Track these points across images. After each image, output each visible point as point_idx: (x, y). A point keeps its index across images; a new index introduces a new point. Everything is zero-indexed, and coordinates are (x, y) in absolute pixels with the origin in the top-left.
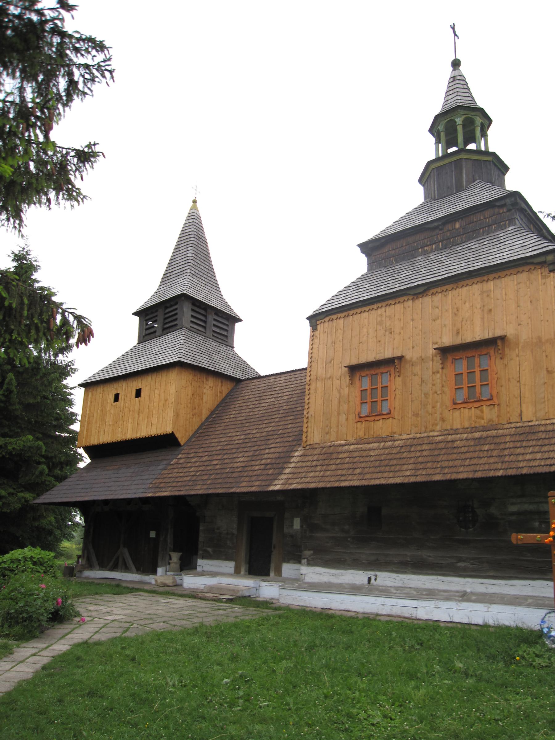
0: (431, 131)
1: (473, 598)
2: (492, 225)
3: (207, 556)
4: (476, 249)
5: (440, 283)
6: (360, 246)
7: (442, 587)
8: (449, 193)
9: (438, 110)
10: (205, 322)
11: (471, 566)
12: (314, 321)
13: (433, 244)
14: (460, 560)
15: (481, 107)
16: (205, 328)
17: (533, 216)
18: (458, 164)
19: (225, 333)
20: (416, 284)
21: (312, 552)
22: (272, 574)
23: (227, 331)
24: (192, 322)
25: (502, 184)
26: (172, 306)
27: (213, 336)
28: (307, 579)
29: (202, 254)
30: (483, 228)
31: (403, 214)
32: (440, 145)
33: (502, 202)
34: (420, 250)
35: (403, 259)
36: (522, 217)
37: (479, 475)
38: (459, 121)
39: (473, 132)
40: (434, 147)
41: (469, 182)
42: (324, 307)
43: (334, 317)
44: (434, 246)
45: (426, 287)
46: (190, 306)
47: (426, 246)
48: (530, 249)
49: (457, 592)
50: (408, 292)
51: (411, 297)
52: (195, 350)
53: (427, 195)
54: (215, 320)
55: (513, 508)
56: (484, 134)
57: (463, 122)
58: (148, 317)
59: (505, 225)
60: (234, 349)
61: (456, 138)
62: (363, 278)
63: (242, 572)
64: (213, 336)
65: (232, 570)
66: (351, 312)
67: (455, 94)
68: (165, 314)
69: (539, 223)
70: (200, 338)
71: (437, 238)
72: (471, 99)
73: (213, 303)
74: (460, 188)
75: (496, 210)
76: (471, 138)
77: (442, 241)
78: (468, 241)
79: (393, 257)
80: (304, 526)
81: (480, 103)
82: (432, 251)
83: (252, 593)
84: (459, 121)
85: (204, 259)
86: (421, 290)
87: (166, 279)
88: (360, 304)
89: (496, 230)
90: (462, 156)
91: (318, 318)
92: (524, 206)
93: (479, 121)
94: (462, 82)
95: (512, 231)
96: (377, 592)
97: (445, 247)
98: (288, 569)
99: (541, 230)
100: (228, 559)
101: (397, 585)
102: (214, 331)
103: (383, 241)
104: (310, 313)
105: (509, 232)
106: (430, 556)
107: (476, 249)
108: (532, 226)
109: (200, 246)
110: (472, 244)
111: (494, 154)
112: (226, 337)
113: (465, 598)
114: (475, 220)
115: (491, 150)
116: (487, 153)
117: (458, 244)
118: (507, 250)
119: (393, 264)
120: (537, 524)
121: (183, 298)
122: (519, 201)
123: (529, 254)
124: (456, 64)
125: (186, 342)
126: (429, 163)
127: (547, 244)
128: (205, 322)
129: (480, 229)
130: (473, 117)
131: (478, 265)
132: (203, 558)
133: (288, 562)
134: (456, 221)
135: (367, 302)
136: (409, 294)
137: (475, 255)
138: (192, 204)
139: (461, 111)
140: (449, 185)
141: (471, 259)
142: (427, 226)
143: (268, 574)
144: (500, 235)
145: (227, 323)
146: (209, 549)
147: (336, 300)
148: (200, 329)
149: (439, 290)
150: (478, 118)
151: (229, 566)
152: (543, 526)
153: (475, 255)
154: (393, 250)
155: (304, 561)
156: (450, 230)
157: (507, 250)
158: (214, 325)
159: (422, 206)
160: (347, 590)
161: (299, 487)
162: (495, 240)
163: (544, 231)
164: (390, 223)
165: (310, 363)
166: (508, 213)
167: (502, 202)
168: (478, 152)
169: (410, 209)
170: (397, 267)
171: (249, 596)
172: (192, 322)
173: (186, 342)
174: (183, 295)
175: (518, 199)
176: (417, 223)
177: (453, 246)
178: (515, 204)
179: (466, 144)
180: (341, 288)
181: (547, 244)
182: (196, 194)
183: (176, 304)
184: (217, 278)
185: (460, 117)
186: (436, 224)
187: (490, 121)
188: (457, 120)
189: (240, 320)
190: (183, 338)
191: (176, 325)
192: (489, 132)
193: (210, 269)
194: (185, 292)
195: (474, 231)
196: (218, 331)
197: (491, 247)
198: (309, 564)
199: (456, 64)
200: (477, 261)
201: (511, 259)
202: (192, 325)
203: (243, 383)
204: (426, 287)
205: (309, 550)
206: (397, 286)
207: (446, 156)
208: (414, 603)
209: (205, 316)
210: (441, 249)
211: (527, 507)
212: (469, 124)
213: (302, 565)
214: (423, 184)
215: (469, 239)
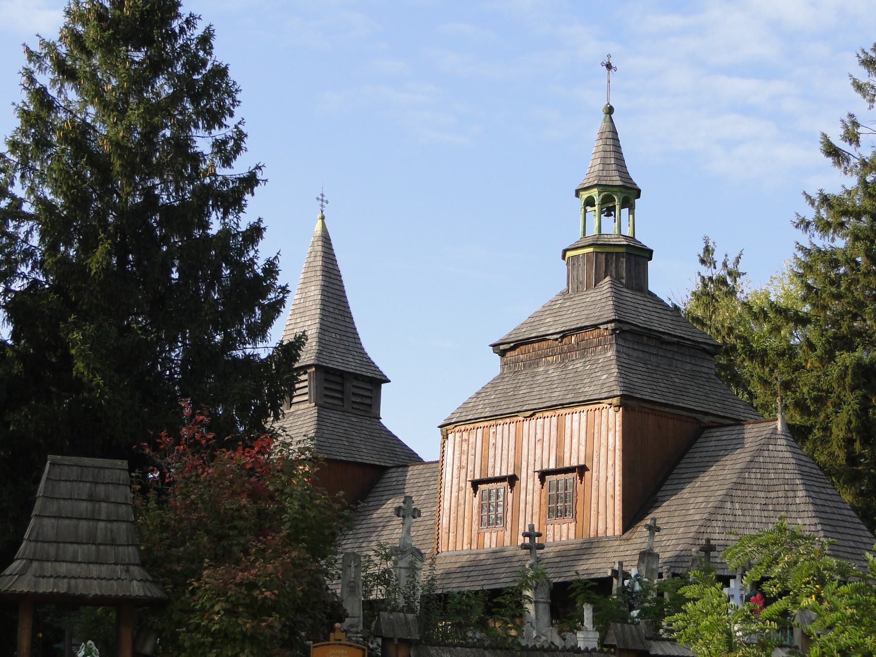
6: (494, 346)
12: (444, 429)
16: (342, 399)
17: (643, 331)
19: (368, 401)
23: (371, 398)
24: (326, 396)
27: (353, 408)
29: (335, 296)
43: (463, 428)
45: (532, 412)
52: (330, 436)
54: (355, 386)
62: (493, 384)
64: (353, 408)
66: (477, 425)
69: (655, 333)
70: (335, 416)
71: (557, 349)
73: (352, 366)
77: (560, 354)
99: (660, 337)
102: (353, 402)
108: (645, 338)
109: (331, 286)
112: (370, 405)
128: (342, 392)
142: (547, 337)
148: (336, 402)
149: (540, 415)
158: (354, 394)
163: (666, 337)
167: (605, 326)
172: (326, 396)
182: (322, 206)
186: (555, 337)
187: (639, 191)
189: (389, 381)
193: (346, 314)
196: (359, 400)
199: (610, 110)
204: (532, 412)
209: (342, 385)
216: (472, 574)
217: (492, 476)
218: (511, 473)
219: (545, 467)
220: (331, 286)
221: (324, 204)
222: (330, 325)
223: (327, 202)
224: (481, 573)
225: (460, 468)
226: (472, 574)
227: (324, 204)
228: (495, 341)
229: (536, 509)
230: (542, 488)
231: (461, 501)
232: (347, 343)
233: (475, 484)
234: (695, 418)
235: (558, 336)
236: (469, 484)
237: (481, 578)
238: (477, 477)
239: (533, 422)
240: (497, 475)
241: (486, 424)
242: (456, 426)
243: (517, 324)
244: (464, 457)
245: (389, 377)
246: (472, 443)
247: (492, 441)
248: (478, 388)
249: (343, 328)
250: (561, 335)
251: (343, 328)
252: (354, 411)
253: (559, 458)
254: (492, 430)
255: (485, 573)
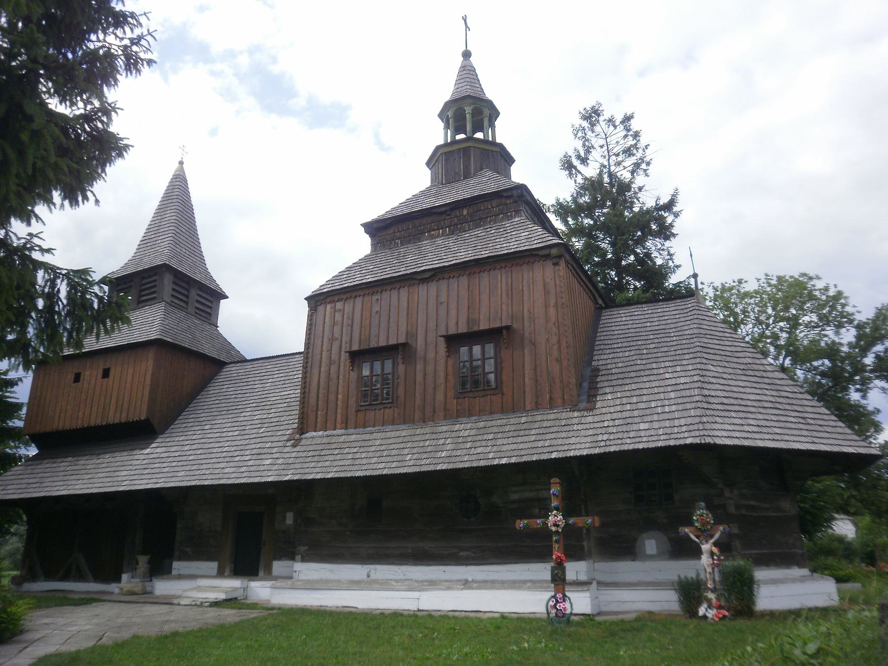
0: (441, 116)
1: (475, 585)
2: (499, 215)
3: (186, 557)
4: (483, 237)
5: (447, 269)
7: (443, 576)
8: (457, 179)
9: (447, 96)
10: (187, 297)
11: (473, 555)
13: (439, 229)
14: (462, 549)
15: (490, 98)
16: (187, 303)
18: (466, 151)
19: (208, 310)
20: (422, 269)
21: (306, 547)
22: (261, 573)
23: (211, 308)
24: (173, 296)
25: (508, 176)
26: (150, 277)
27: (196, 313)
28: (302, 577)
30: (490, 217)
31: (410, 196)
32: (449, 132)
33: (509, 193)
34: (427, 234)
35: (409, 242)
36: (528, 209)
37: (483, 463)
38: (468, 110)
39: (482, 121)
40: (442, 132)
41: (476, 171)
42: (325, 287)
43: (336, 298)
44: (441, 231)
45: (432, 273)
46: (172, 277)
47: (433, 231)
48: (536, 242)
49: (459, 581)
50: (414, 277)
51: (417, 282)
52: (176, 327)
53: (434, 179)
54: (198, 295)
55: (515, 497)
56: (492, 125)
57: (472, 110)
58: (119, 288)
59: (511, 216)
60: (218, 328)
61: (466, 126)
62: (366, 259)
63: (226, 574)
64: (196, 313)
65: (214, 571)
67: (466, 83)
68: (142, 285)
70: (181, 314)
71: (444, 223)
72: (480, 90)
74: (467, 176)
75: (503, 200)
76: (478, 127)
78: (476, 228)
79: (398, 239)
80: (299, 521)
81: (490, 94)
82: (438, 236)
83: (239, 594)
84: (468, 110)
85: (188, 226)
86: (427, 275)
87: (145, 245)
88: (363, 286)
89: (502, 220)
90: (469, 144)
91: (317, 299)
92: (529, 198)
93: (486, 112)
94: (471, 73)
95: (518, 223)
96: (377, 586)
97: (452, 233)
98: (278, 567)
99: (545, 223)
100: (210, 558)
101: (397, 577)
103: (388, 222)
104: (309, 293)
105: (515, 223)
106: (431, 547)
107: (483, 237)
109: (185, 213)
110: (479, 232)
111: (501, 146)
113: (467, 586)
114: (482, 208)
115: (498, 141)
116: (494, 143)
117: (465, 231)
118: (513, 240)
119: (398, 246)
120: (537, 510)
121: (164, 269)
122: (525, 193)
123: (534, 247)
124: (467, 55)
125: (166, 317)
126: (438, 148)
127: (551, 238)
128: (187, 297)
129: (488, 217)
130: (482, 107)
131: (485, 254)
132: (179, 559)
133: (279, 559)
134: (463, 207)
135: (371, 285)
136: (415, 279)
137: (483, 244)
138: (177, 165)
139: (470, 101)
140: (457, 170)
141: (479, 247)
142: (434, 211)
143: (257, 575)
144: (507, 226)
145: (211, 299)
146: (188, 550)
147: (337, 281)
148: (182, 304)
150: (487, 109)
151: (213, 566)
152: (543, 512)
153: (483, 244)
154: (398, 231)
155: (298, 557)
156: (457, 216)
157: (513, 240)
158: (198, 301)
159: (428, 190)
160: (345, 585)
161: (296, 478)
162: (502, 230)
164: (396, 204)
165: (307, 345)
166: (514, 204)
168: (485, 141)
169: (416, 192)
170: (402, 250)
171: (236, 598)
173: (166, 317)
174: (165, 265)
175: (524, 192)
176: (425, 206)
177: (460, 232)
178: (521, 196)
179: (474, 133)
180: (343, 269)
181: (551, 238)
182: (183, 154)
183: (155, 274)
184: (203, 249)
185: (470, 106)
186: (444, 209)
187: (497, 114)
188: (466, 108)
189: (227, 297)
190: (163, 313)
191: (154, 298)
192: (498, 123)
193: (195, 238)
194: (167, 263)
195: (481, 219)
196: (201, 307)
197: (498, 237)
198: (304, 560)
199: (467, 55)
200: (484, 249)
201: (518, 249)
202: (173, 299)
203: (228, 366)
205: (304, 545)
206: (403, 269)
207: (454, 142)
208: (416, 594)
209: (188, 290)
210: (448, 235)
211: (527, 495)
212: (477, 113)
213: (296, 562)
214: (430, 167)
215: (477, 226)
216: (358, 456)
217: (376, 346)
218: (402, 340)
219: (452, 331)
220: (184, 212)
221: (185, 154)
222: (181, 241)
223: (187, 153)
224: (370, 454)
225: (332, 339)
226: (358, 456)
227: (185, 154)
228: (369, 219)
229: (441, 380)
230: (448, 356)
231: (333, 375)
232: (194, 259)
233: (357, 357)
234: (594, 296)
235: (448, 208)
236: (345, 356)
237: (373, 460)
238: (355, 347)
239: (433, 286)
240: (383, 343)
241: (367, 292)
242: (328, 297)
243: (389, 209)
244: (337, 329)
245: (227, 294)
246: (348, 313)
247: (376, 308)
248: (350, 264)
249: (192, 248)
250: (451, 206)
251: (192, 248)
252: (196, 315)
253: (469, 321)
254: (375, 297)
255: (378, 454)
